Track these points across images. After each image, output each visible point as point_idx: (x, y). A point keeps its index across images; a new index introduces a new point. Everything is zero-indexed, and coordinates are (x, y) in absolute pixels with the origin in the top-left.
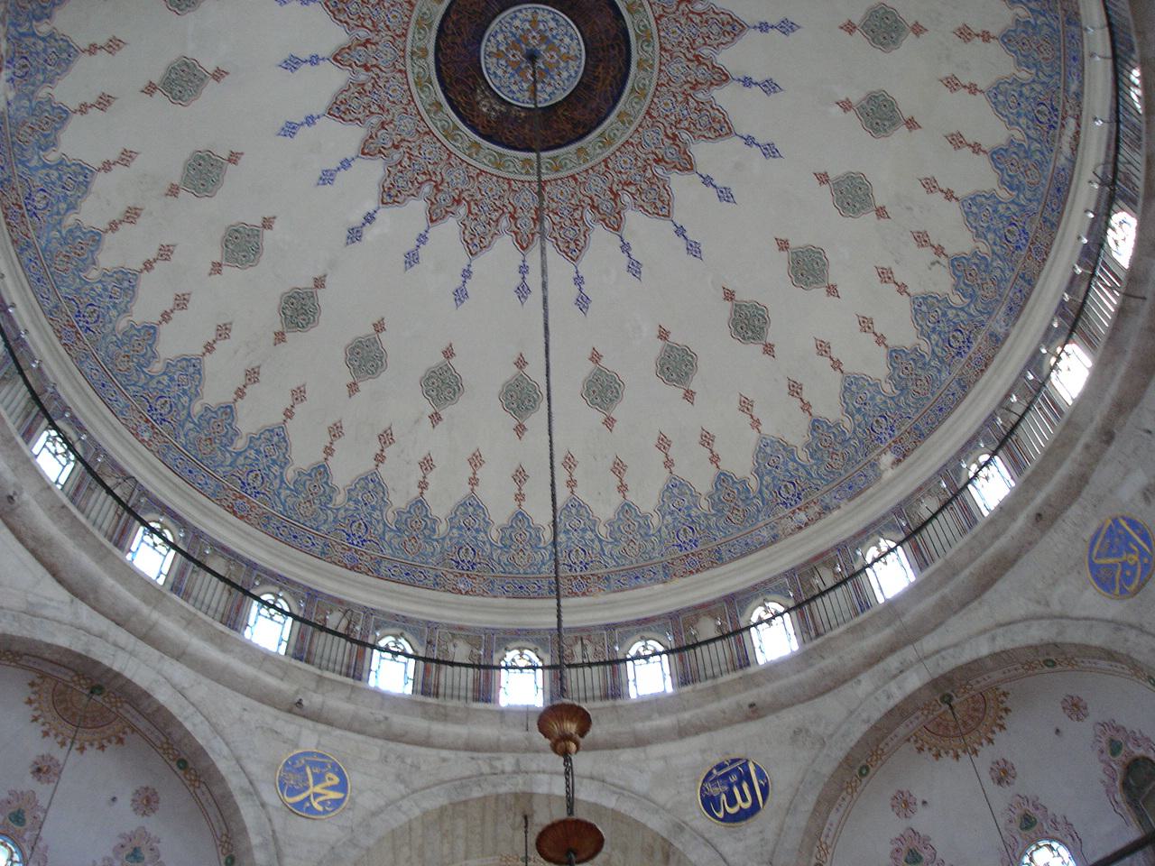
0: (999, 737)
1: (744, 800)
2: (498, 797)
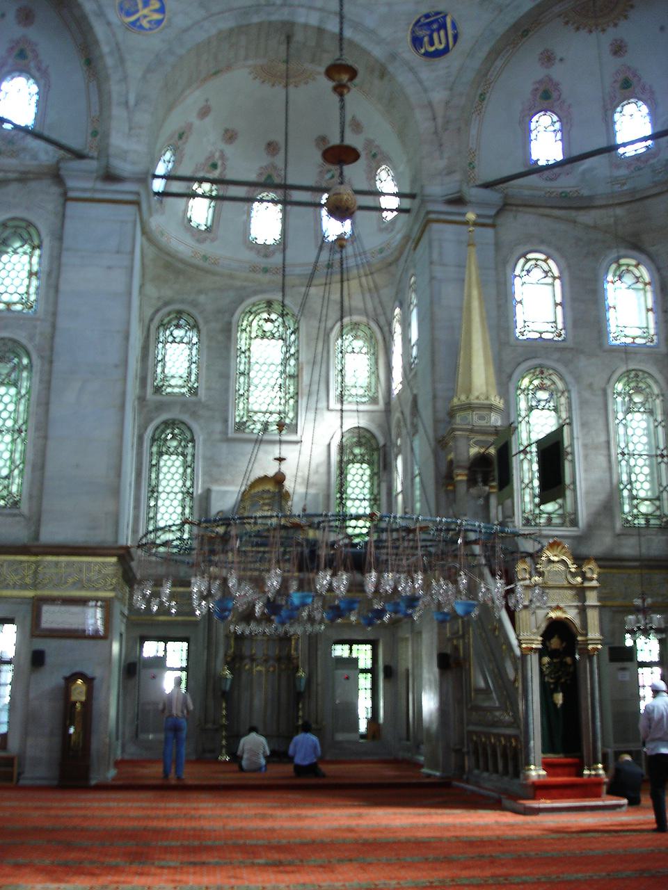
0: (623, 24)
1: (441, 43)
2: (270, 23)
